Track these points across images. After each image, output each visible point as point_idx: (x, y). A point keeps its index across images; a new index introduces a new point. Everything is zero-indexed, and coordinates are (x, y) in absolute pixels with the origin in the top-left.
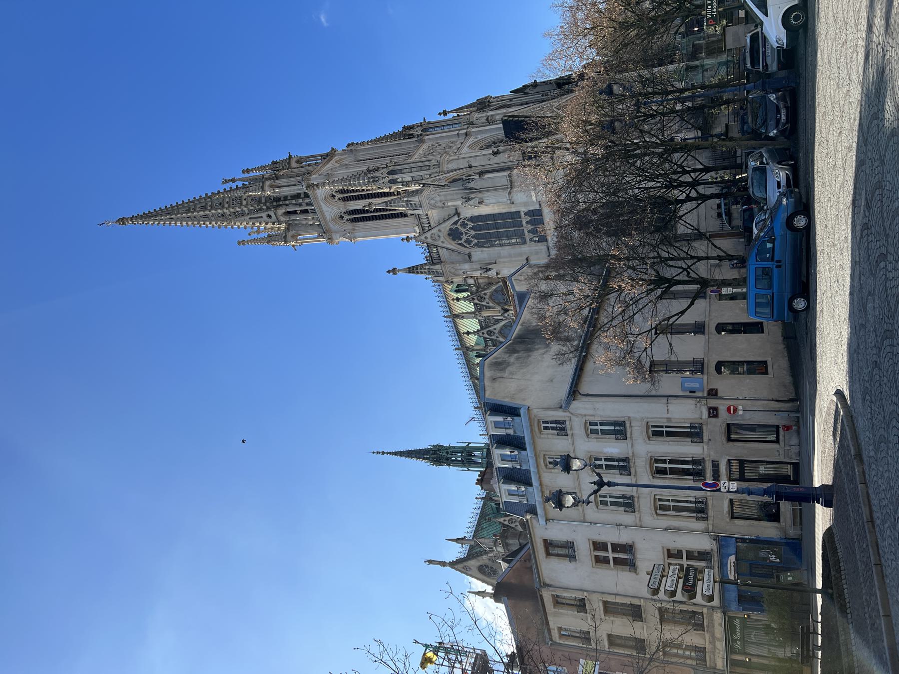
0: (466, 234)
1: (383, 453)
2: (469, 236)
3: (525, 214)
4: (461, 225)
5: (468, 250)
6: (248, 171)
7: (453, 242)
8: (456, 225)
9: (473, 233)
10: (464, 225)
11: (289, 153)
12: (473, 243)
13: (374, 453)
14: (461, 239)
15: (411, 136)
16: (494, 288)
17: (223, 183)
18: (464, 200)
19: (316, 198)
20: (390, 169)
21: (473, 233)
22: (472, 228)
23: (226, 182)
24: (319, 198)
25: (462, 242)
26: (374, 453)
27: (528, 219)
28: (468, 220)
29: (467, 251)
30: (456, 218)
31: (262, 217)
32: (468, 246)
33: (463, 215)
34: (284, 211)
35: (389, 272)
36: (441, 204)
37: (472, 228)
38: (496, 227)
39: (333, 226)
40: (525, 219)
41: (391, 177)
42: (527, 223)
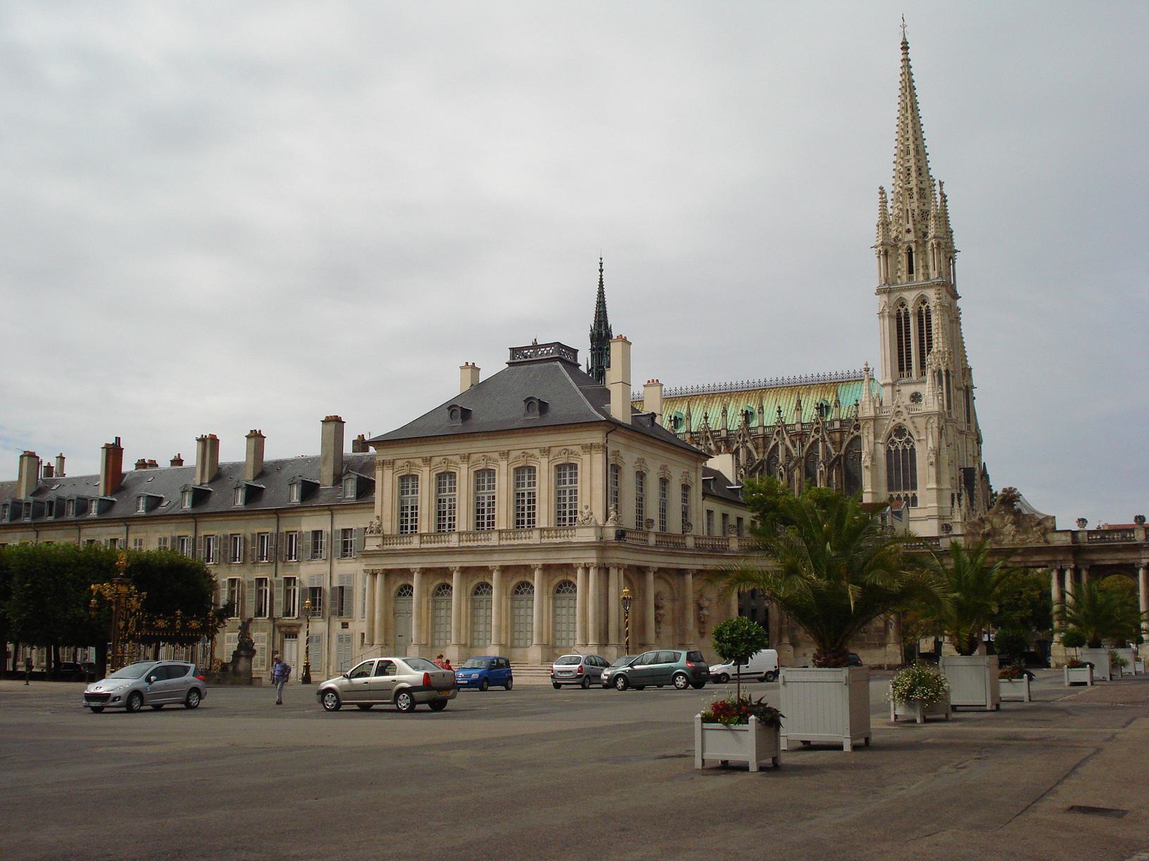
1: (601, 271)
13: (601, 259)
14: (895, 436)
15: (964, 375)
17: (940, 182)
20: (951, 373)
22: (904, 450)
25: (893, 437)
26: (601, 259)
28: (912, 446)
30: (916, 437)
31: (908, 223)
36: (929, 426)
39: (896, 295)
41: (944, 373)
42: (907, 494)
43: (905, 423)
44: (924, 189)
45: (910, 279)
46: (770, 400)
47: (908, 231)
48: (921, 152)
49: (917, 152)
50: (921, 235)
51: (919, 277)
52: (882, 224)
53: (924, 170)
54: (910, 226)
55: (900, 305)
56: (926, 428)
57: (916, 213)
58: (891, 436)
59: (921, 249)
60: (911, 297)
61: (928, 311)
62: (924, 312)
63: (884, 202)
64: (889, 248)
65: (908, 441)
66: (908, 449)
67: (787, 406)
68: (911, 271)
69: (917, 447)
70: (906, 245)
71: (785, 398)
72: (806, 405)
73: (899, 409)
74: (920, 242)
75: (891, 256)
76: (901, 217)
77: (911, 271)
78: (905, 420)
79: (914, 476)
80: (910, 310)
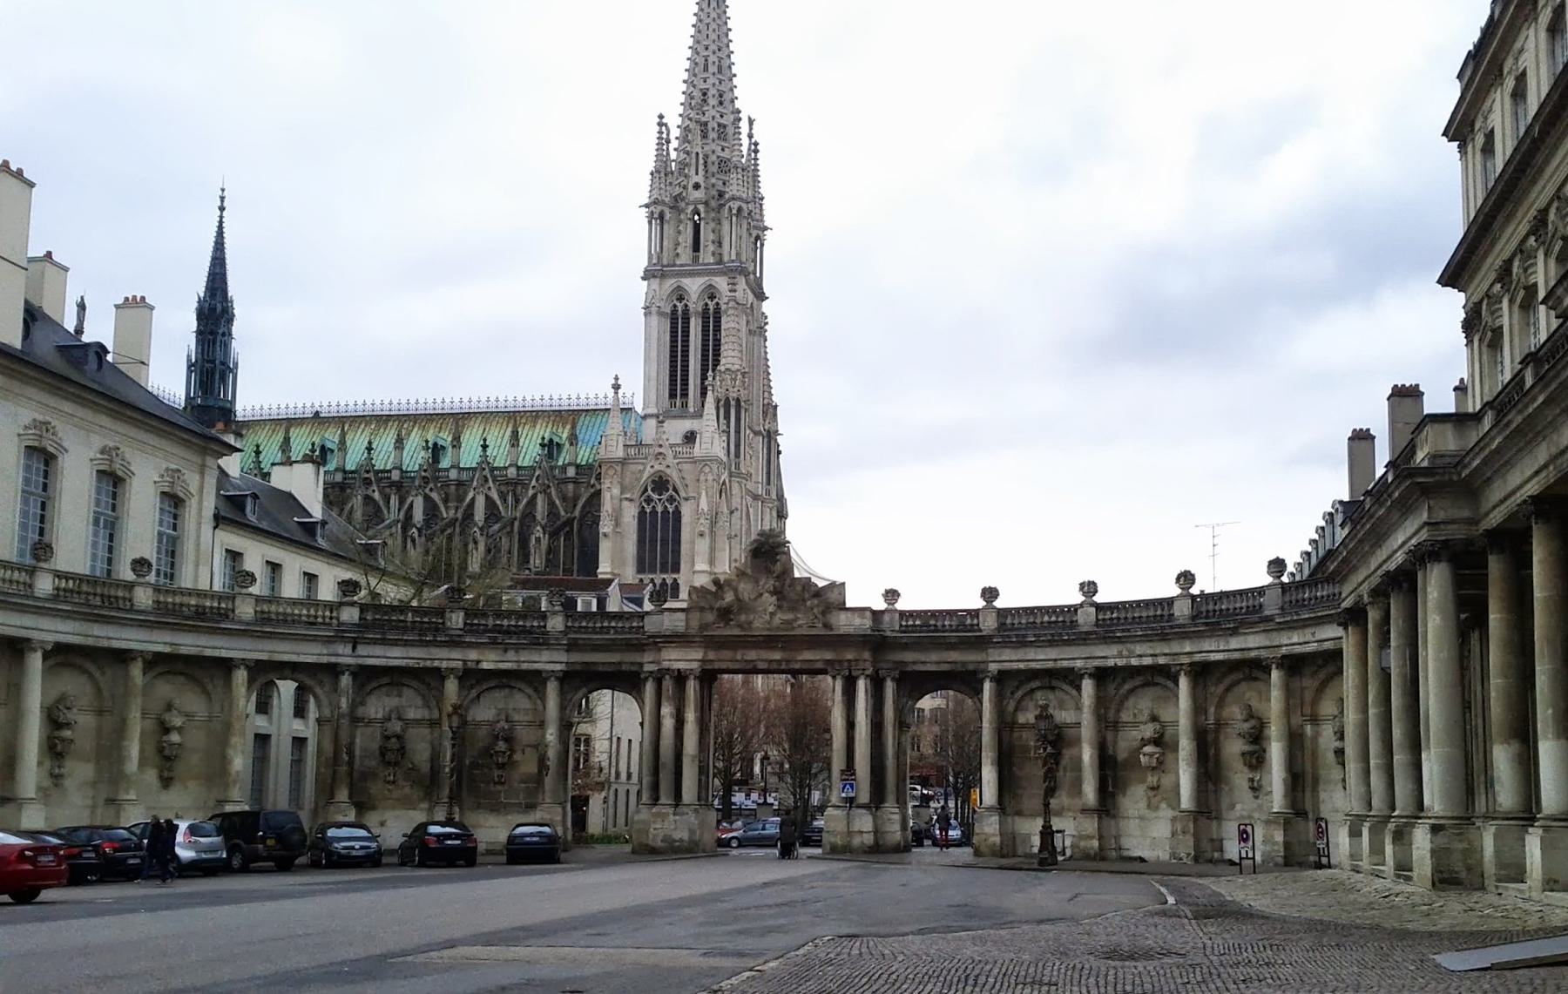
0: (660, 500)
1: (222, 209)
3: (675, 579)
4: (672, 496)
6: (756, 151)
9: (660, 509)
10: (671, 500)
13: (223, 190)
14: (653, 490)
15: (765, 414)
16: (557, 502)
17: (750, 118)
20: (743, 404)
21: (660, 509)
22: (665, 511)
23: (751, 122)
26: (223, 190)
27: (669, 582)
29: (636, 496)
30: (683, 494)
31: (697, 174)
32: (642, 499)
35: (617, 378)
36: (702, 478)
37: (666, 507)
38: (664, 541)
39: (670, 283)
40: (669, 578)
42: (664, 579)
43: (668, 471)
44: (725, 127)
45: (696, 260)
46: (475, 430)
47: (697, 186)
48: (725, 70)
50: (714, 193)
51: (707, 256)
52: (658, 171)
53: (727, 97)
54: (700, 179)
55: (677, 299)
56: (698, 480)
57: (709, 161)
58: (646, 490)
60: (694, 286)
61: (717, 311)
62: (711, 311)
63: (663, 141)
64: (667, 211)
65: (671, 500)
66: (671, 510)
67: (499, 440)
68: (696, 247)
69: (686, 510)
71: (498, 429)
72: (527, 442)
73: (661, 450)
74: (713, 204)
75: (669, 222)
76: (687, 165)
77: (696, 247)
80: (691, 306)
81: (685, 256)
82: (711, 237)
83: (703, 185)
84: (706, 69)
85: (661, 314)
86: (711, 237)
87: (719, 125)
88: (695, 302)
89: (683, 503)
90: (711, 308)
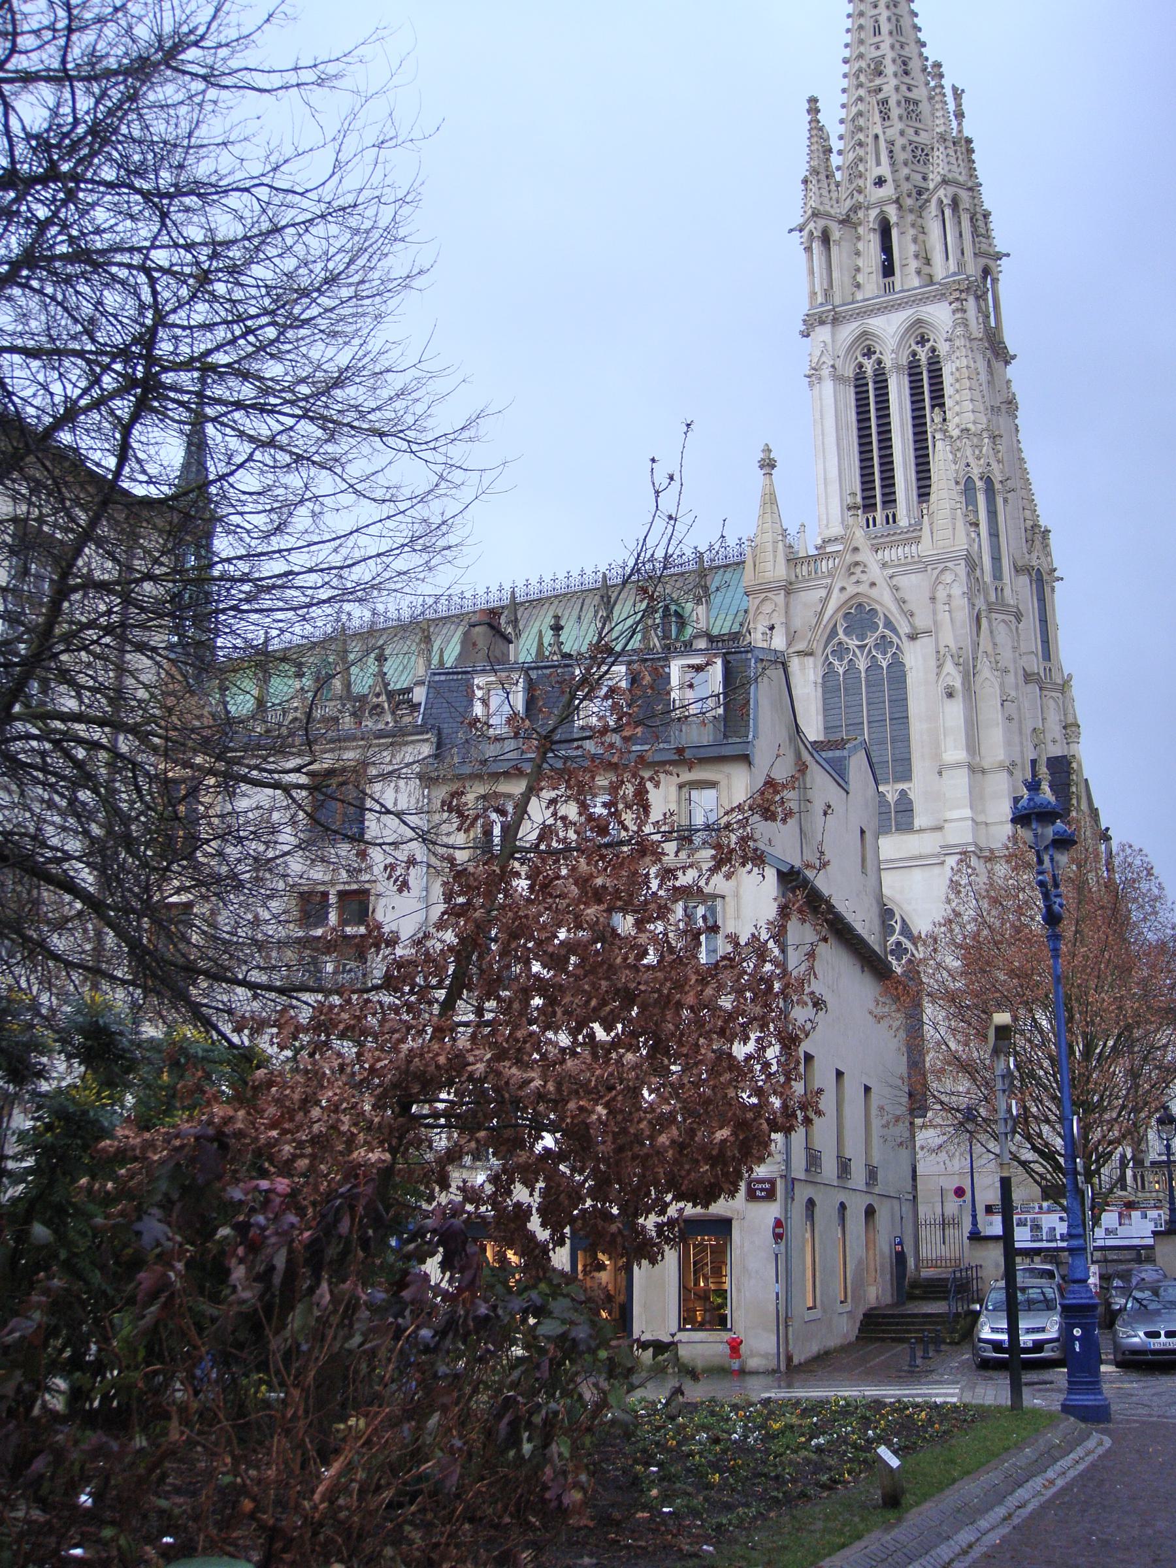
2: (854, 654)
3: (903, 793)
5: (820, 651)
7: (840, 614)
8: (885, 627)
9: (862, 664)
11: (1008, 255)
12: (836, 663)
14: (847, 632)
17: (955, 89)
18: (954, 650)
19: (923, 300)
20: (998, 486)
21: (862, 664)
22: (874, 666)
24: (923, 309)
29: (818, 647)
30: (904, 629)
31: (878, 164)
32: (829, 650)
33: (906, 645)
34: (893, 219)
36: (941, 594)
39: (848, 331)
41: (979, 484)
43: (874, 592)
44: (916, 103)
45: (889, 289)
47: (880, 182)
49: (898, 30)
51: (907, 278)
52: (815, 171)
56: (933, 599)
57: (897, 148)
58: (833, 633)
59: (910, 218)
63: (817, 130)
64: (834, 228)
65: (883, 644)
68: (888, 270)
70: (873, 213)
74: (909, 202)
75: (838, 243)
77: (888, 270)
78: (873, 584)
79: (902, 739)
81: (872, 283)
82: (912, 248)
83: (889, 176)
84: (877, 31)
85: (838, 378)
86: (912, 248)
87: (907, 100)
88: (892, 352)
89: (906, 645)
90: (924, 361)
